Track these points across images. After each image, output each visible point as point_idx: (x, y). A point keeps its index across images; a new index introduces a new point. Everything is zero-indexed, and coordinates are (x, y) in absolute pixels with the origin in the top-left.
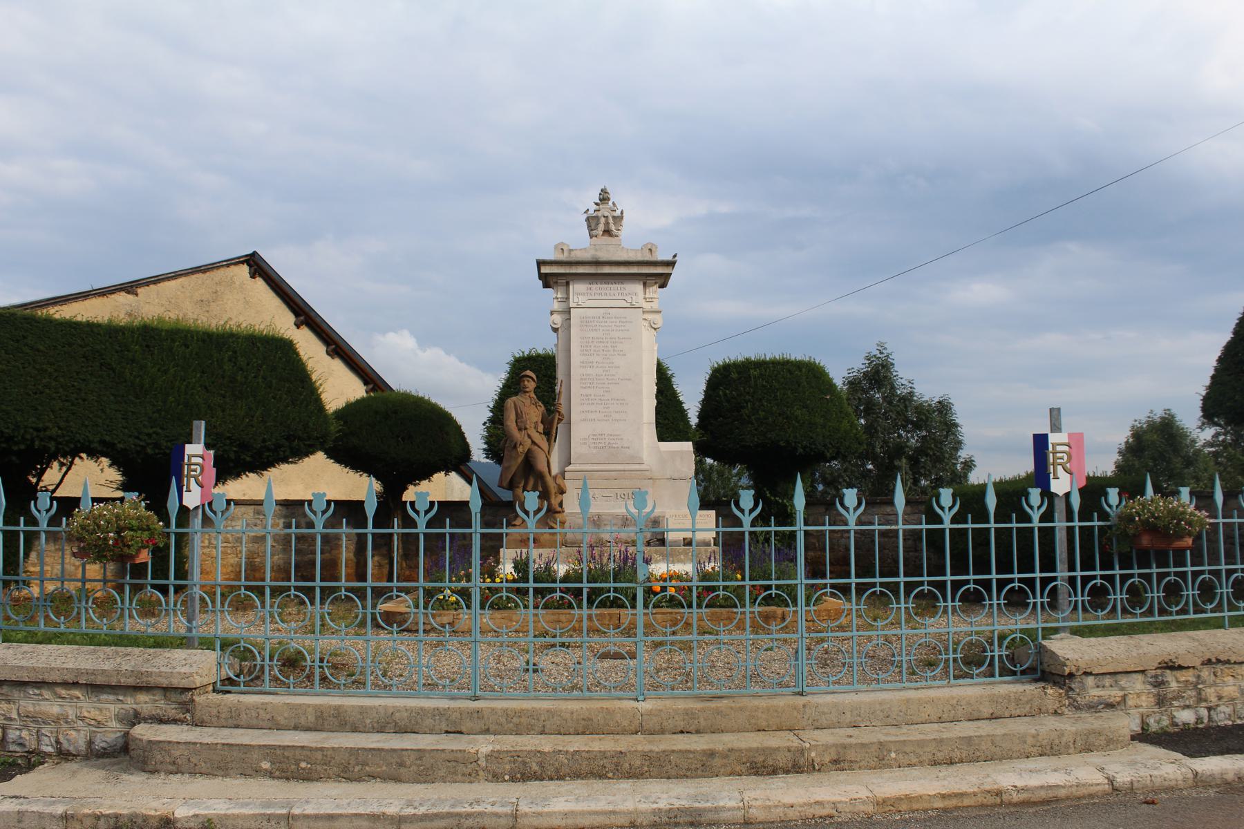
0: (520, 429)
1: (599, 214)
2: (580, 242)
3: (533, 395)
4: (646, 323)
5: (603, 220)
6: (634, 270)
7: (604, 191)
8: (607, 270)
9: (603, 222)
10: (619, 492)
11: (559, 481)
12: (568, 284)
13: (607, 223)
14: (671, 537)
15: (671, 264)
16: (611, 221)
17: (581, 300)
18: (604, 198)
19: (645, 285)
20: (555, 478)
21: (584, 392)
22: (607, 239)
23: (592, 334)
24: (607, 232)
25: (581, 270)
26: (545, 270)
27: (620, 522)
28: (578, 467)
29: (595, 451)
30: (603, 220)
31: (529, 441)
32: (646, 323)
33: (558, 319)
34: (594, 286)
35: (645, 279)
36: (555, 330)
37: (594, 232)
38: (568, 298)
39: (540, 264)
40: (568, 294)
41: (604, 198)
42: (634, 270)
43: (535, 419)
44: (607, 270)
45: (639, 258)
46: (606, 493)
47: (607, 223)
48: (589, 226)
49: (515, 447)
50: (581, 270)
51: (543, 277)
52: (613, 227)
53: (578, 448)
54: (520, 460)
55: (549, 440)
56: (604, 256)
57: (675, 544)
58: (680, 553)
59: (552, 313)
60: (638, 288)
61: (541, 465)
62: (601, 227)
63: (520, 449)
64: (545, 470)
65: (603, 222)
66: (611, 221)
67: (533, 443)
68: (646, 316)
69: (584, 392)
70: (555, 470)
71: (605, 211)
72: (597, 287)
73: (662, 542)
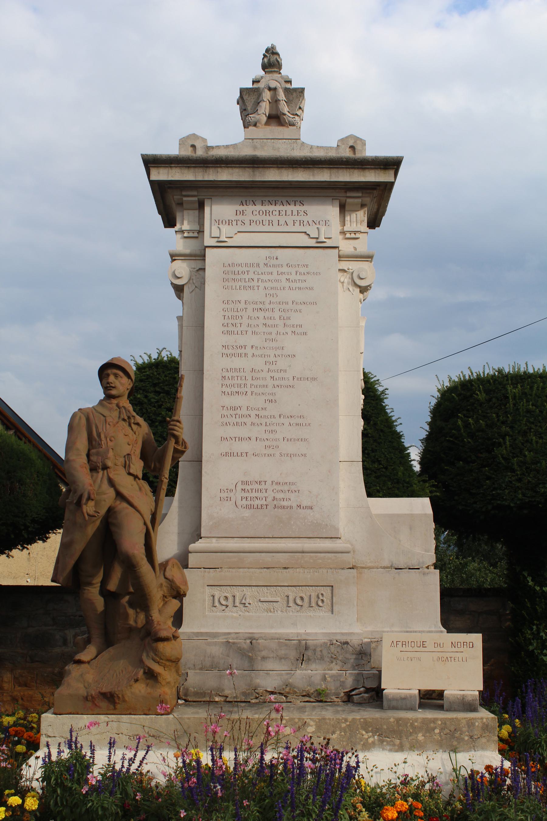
0: (93, 469)
1: (261, 85)
2: (225, 132)
3: (125, 403)
4: (345, 278)
5: (267, 95)
6: (324, 176)
7: (271, 52)
8: (272, 175)
9: (270, 98)
10: (292, 593)
11: (173, 572)
12: (201, 206)
13: (275, 102)
14: (391, 686)
15: (393, 164)
16: (282, 96)
17: (226, 231)
18: (271, 62)
19: (343, 208)
20: (164, 566)
21: (229, 401)
22: (276, 131)
23: (244, 295)
24: (276, 118)
25: (225, 175)
26: (161, 175)
27: (293, 654)
28: (214, 544)
29: (247, 513)
30: (267, 95)
31: (111, 493)
32: (345, 278)
33: (183, 269)
34: (249, 208)
35: (343, 195)
36: (179, 290)
37: (252, 118)
38: (201, 232)
39: (151, 162)
40: (201, 224)
41: (271, 62)
42: (324, 176)
43: (127, 449)
44: (272, 175)
45: (332, 154)
46: (267, 594)
47: (275, 102)
48: (244, 113)
49: (79, 504)
50: (225, 175)
51: (161, 190)
52: (285, 108)
53: (214, 508)
54: (91, 530)
55: (155, 490)
56: (265, 152)
57: (401, 704)
58: (416, 730)
59: (174, 257)
60: (330, 211)
61: (132, 541)
62: (265, 108)
63: (89, 508)
64: (138, 550)
65: (270, 98)
66: (282, 96)
67: (119, 495)
68: (344, 265)
69: (229, 401)
70: (167, 546)
71: (272, 80)
72: (254, 211)
73: (375, 695)
